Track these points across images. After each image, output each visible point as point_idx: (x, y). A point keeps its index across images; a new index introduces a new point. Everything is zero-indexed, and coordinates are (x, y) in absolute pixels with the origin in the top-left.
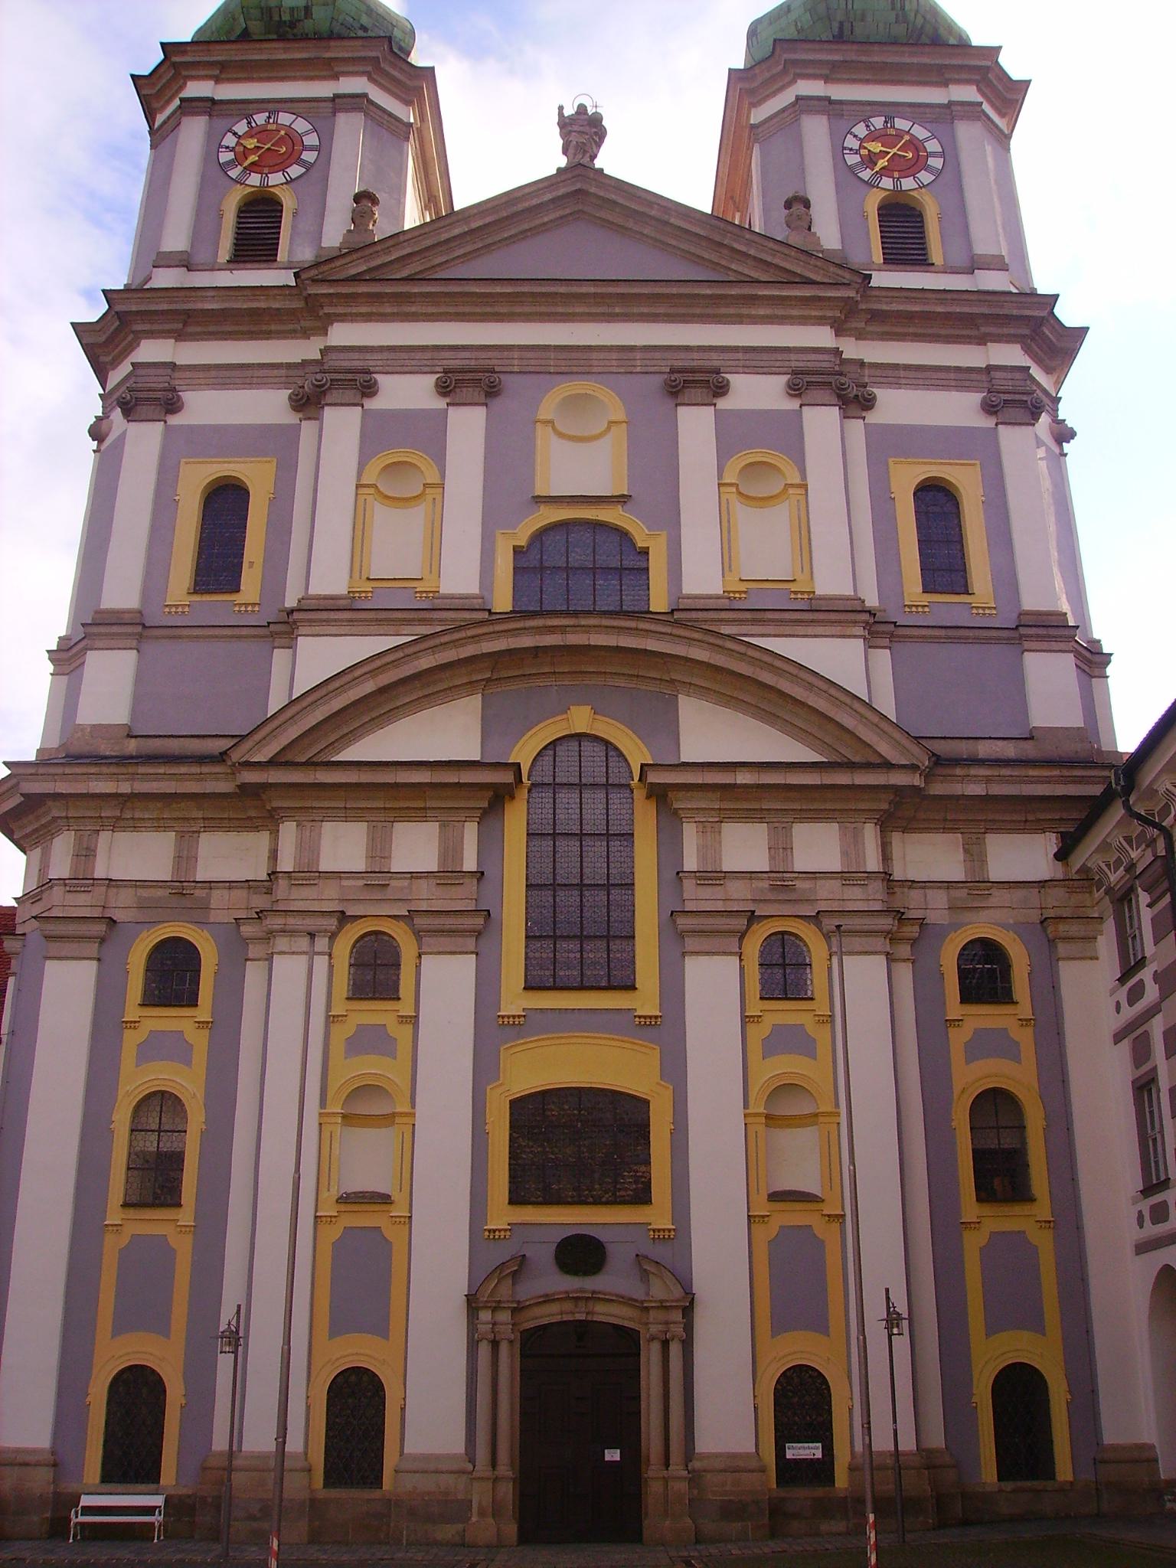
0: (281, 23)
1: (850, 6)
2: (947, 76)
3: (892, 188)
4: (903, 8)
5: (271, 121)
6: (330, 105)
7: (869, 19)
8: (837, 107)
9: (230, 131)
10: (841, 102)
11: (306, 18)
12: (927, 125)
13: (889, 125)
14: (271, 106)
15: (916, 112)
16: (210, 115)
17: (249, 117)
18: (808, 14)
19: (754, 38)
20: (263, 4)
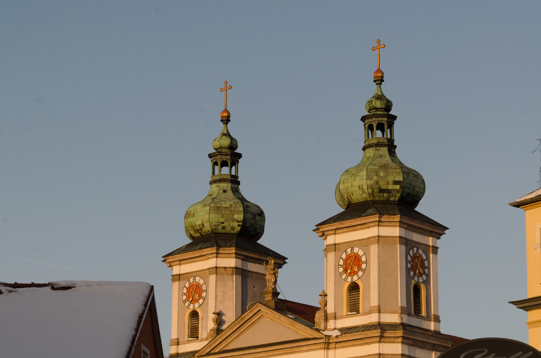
1: (347, 191)
7: (355, 194)
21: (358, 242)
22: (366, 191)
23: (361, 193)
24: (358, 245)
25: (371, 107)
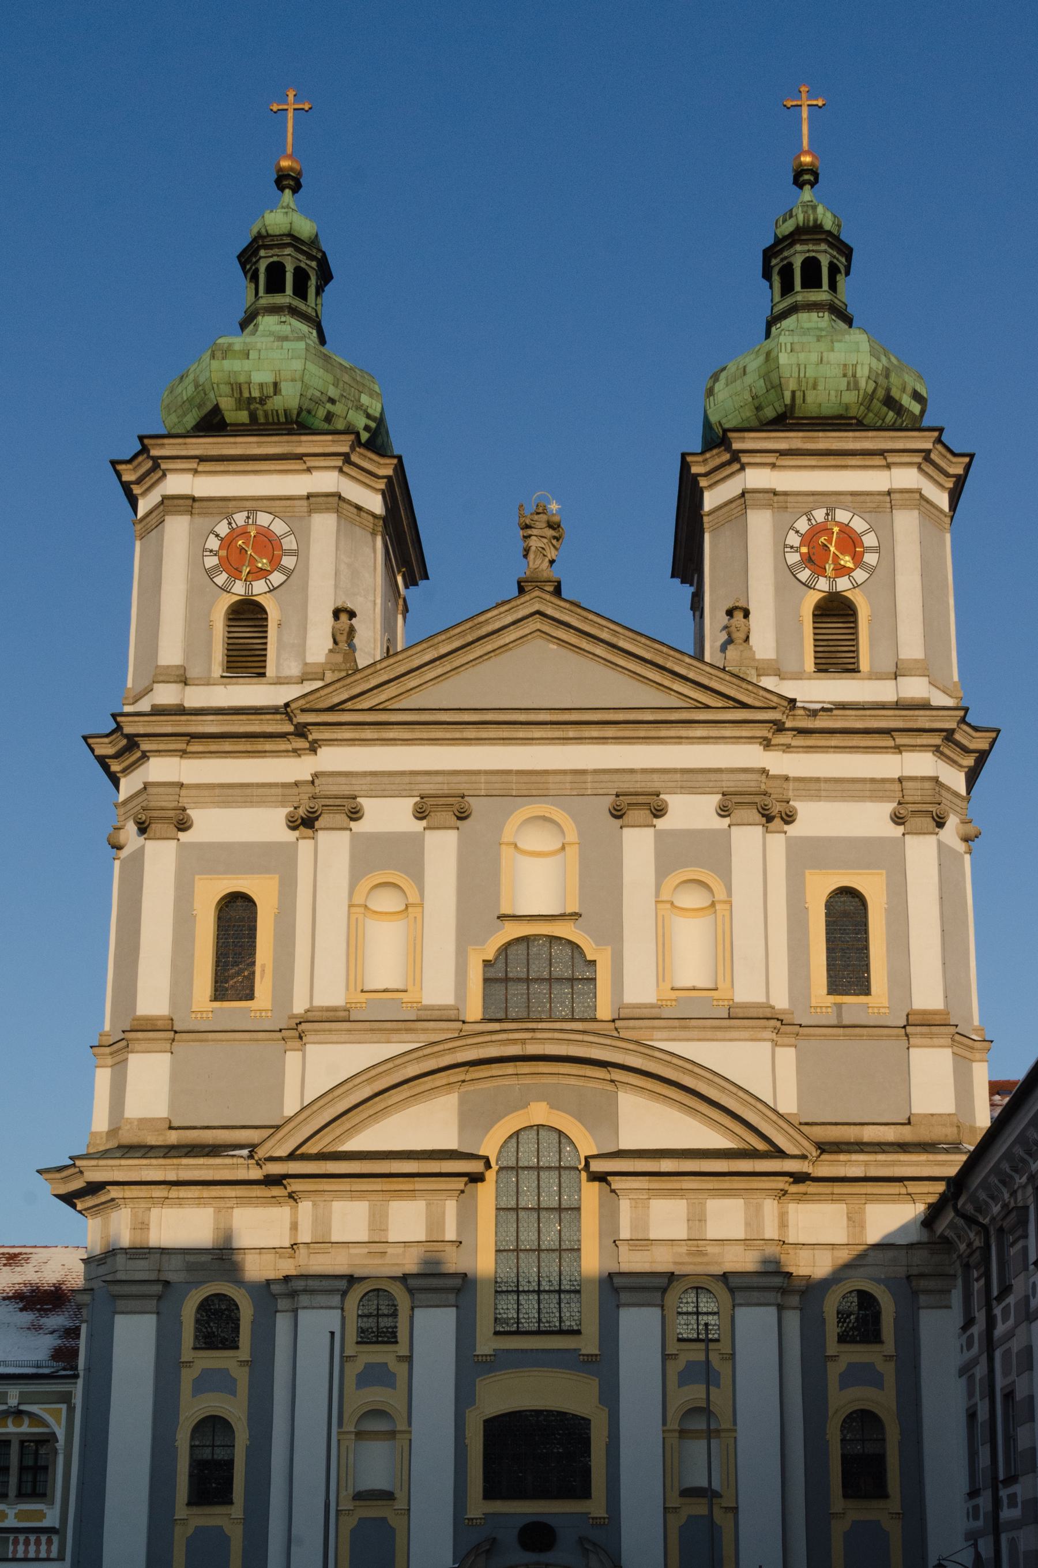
0: (251, 400)
1: (802, 375)
2: (890, 460)
3: (827, 590)
4: (854, 376)
5: (250, 521)
6: (305, 503)
7: (820, 387)
8: (781, 498)
9: (212, 532)
10: (786, 494)
11: (275, 395)
12: (866, 516)
13: (830, 517)
14: (248, 504)
15: (857, 499)
16: (192, 514)
17: (229, 517)
18: (762, 381)
19: (711, 398)
20: (232, 381)
21: (849, 498)
22: (862, 384)
23: (843, 385)
24: (850, 505)
25: (809, 221)
